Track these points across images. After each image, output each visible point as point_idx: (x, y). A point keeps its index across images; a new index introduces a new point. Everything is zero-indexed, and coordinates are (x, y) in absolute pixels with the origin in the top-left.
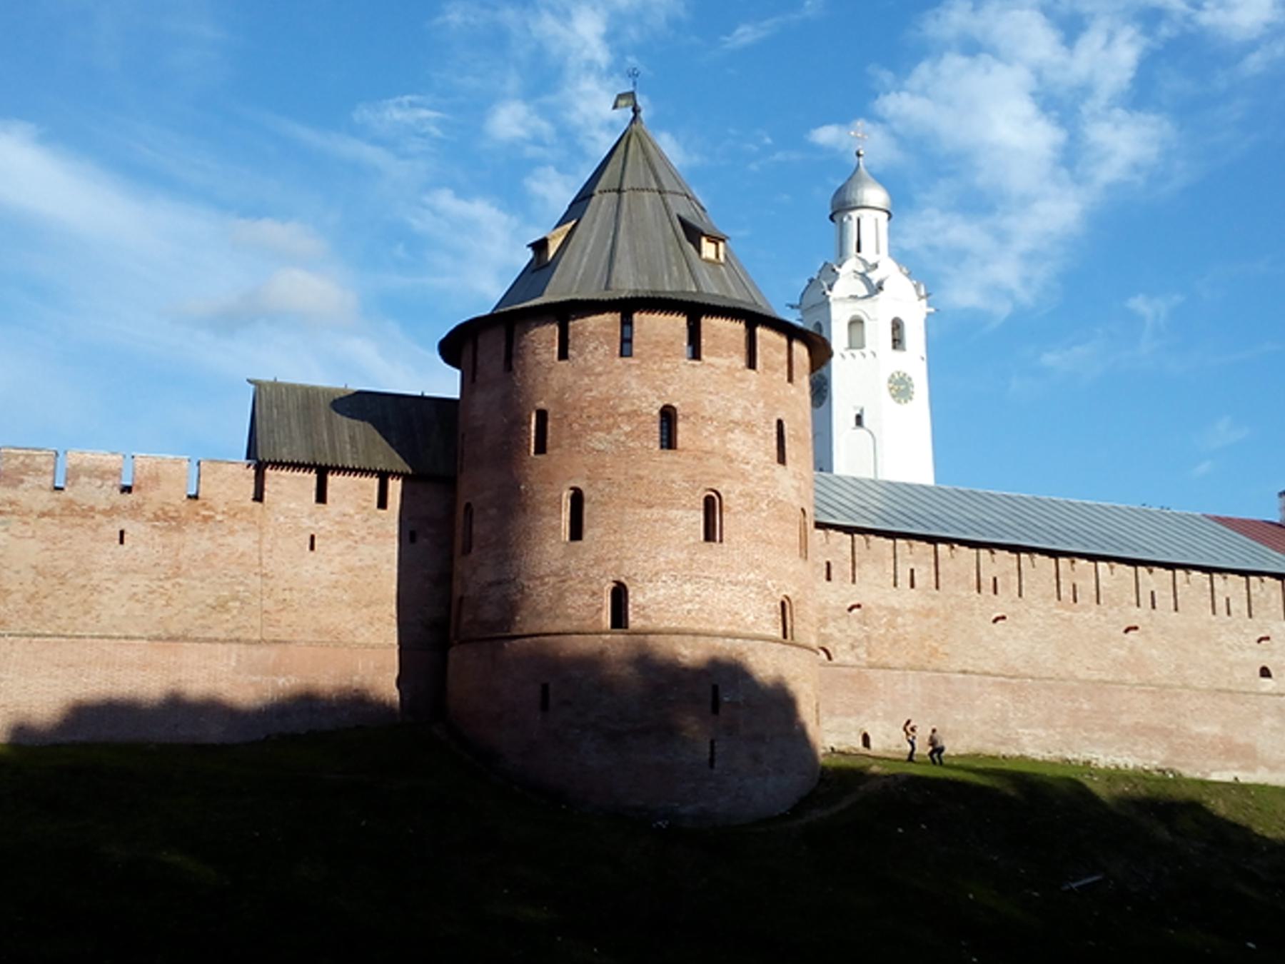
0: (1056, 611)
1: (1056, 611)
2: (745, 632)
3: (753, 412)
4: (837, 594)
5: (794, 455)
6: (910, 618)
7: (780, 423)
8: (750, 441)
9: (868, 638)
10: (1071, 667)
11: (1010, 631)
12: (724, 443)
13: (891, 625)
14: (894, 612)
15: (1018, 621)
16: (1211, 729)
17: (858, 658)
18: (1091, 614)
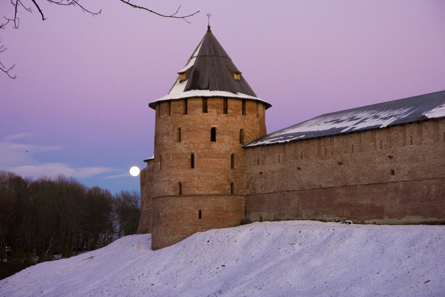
0: (319, 161)
1: (319, 161)
2: (165, 195)
3: (169, 129)
4: (257, 169)
5: (185, 137)
6: (277, 173)
7: (180, 129)
8: (168, 138)
9: (266, 183)
10: (321, 183)
11: (304, 173)
12: (162, 140)
13: (272, 177)
14: (273, 172)
15: (307, 168)
16: (367, 202)
17: (262, 191)
18: (331, 160)
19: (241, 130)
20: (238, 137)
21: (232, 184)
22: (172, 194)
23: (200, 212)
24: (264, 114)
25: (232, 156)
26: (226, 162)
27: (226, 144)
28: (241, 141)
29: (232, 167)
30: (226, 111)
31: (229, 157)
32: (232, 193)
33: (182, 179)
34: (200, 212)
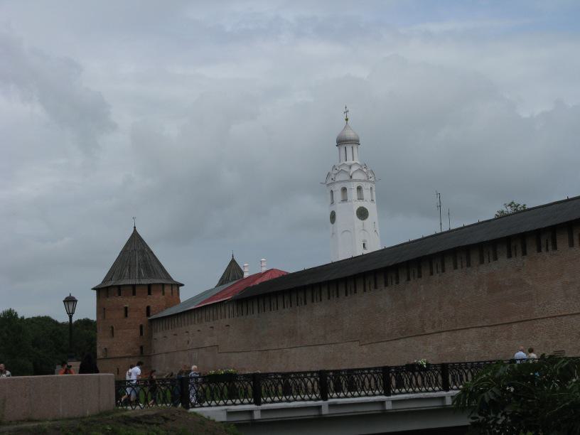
19: (148, 308)
20: (145, 312)
21: (141, 348)
22: (101, 357)
23: (118, 369)
24: (178, 289)
25: (141, 327)
26: (136, 332)
27: (137, 318)
28: (148, 315)
29: (141, 334)
30: (134, 294)
31: (139, 328)
32: (142, 352)
33: (106, 346)
34: (118, 369)
